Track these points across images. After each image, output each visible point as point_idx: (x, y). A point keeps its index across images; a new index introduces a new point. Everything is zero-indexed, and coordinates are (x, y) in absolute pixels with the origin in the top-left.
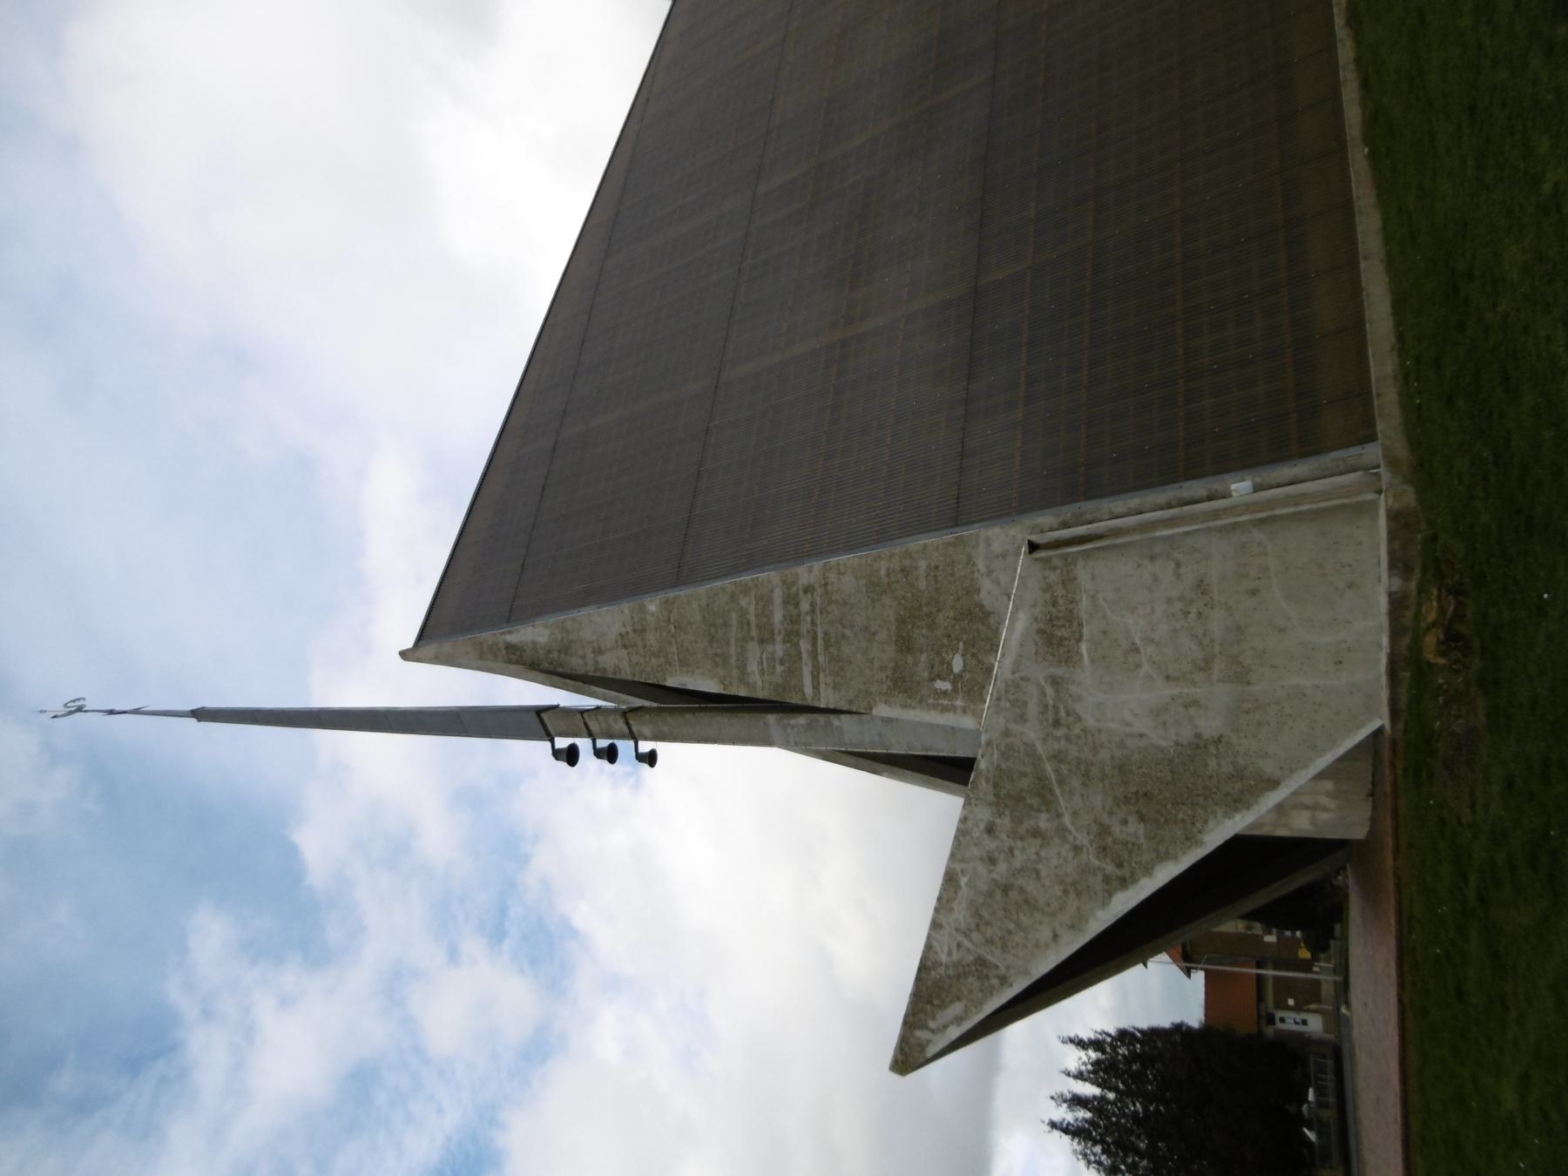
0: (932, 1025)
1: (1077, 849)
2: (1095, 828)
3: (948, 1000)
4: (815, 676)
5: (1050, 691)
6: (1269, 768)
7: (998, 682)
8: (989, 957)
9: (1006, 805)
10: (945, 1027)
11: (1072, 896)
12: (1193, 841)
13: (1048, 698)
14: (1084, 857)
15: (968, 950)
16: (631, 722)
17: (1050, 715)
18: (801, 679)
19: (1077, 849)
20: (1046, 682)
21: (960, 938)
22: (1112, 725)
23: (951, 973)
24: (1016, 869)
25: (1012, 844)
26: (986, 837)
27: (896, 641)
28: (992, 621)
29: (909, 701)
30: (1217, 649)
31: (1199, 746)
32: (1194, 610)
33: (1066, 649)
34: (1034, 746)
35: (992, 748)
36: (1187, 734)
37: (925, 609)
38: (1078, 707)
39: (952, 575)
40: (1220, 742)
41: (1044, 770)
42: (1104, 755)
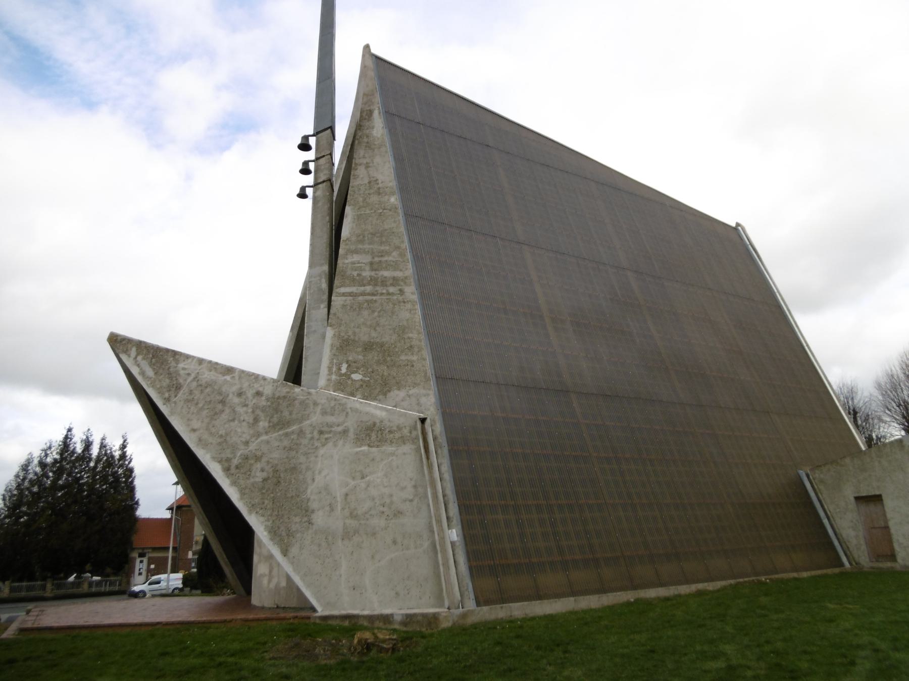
0: (140, 358)
1: (247, 443)
2: (259, 453)
3: (155, 367)
4: (350, 294)
5: (340, 429)
6: (294, 550)
7: (345, 400)
8: (182, 391)
9: (272, 403)
10: (138, 366)
11: (219, 440)
12: (251, 508)
13: (336, 428)
14: (243, 447)
15: (186, 380)
16: (325, 184)
17: (325, 429)
18: (349, 286)
19: (247, 443)
20: (345, 427)
21: (193, 376)
22: (319, 463)
23: (171, 370)
24: (234, 408)
25: (250, 406)
26: (254, 391)
27: (370, 342)
28: (381, 397)
29: (335, 348)
30: (363, 522)
31: (307, 512)
32: (385, 509)
33: (364, 438)
34: (308, 419)
35: (307, 396)
36: (314, 505)
37: (389, 359)
38: (330, 444)
39: (408, 375)
40: (309, 523)
41: (293, 425)
42: (302, 459)
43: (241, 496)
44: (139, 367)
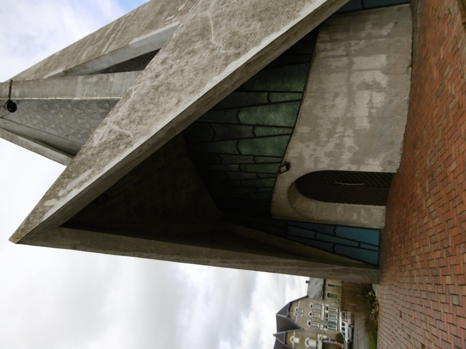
9: (179, 47)
43: (275, 32)
44: (72, 190)
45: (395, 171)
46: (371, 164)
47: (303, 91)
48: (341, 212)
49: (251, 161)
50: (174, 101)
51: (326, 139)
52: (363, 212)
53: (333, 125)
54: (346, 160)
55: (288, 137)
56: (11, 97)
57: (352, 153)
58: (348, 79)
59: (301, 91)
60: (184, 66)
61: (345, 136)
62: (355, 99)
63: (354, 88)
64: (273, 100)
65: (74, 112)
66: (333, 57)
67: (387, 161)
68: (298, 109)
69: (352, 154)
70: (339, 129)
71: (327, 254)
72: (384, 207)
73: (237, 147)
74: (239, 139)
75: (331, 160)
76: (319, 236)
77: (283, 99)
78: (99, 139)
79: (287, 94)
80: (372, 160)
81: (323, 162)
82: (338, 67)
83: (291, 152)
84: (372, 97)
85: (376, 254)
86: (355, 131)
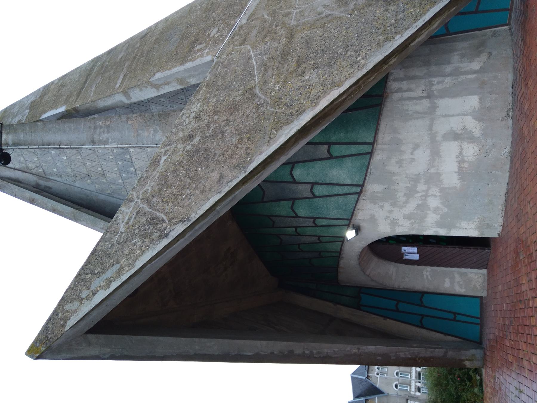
7: (236, 29)
15: (145, 214)
44: (98, 291)
45: (497, 236)
46: (464, 227)
47: (372, 142)
48: (429, 277)
49: (311, 224)
50: (215, 176)
51: (404, 199)
52: (457, 278)
53: (412, 183)
54: (432, 223)
55: (356, 196)
56: (2, 145)
57: (439, 215)
58: (430, 128)
59: (370, 142)
60: (224, 126)
61: (429, 196)
62: (441, 151)
63: (439, 138)
64: (334, 154)
65: (81, 153)
66: (410, 99)
67: (484, 224)
68: (367, 164)
69: (439, 216)
70: (421, 187)
71: (414, 328)
72: (484, 271)
73: (292, 208)
74: (294, 200)
75: (412, 224)
76: (401, 306)
77: (348, 152)
78: (125, 221)
79: (353, 146)
80: (465, 223)
81: (402, 226)
82: (417, 112)
83: (360, 214)
84: (462, 149)
85: (478, 327)
86: (441, 190)
